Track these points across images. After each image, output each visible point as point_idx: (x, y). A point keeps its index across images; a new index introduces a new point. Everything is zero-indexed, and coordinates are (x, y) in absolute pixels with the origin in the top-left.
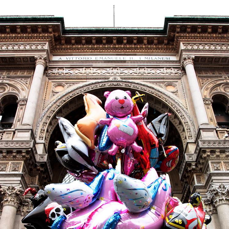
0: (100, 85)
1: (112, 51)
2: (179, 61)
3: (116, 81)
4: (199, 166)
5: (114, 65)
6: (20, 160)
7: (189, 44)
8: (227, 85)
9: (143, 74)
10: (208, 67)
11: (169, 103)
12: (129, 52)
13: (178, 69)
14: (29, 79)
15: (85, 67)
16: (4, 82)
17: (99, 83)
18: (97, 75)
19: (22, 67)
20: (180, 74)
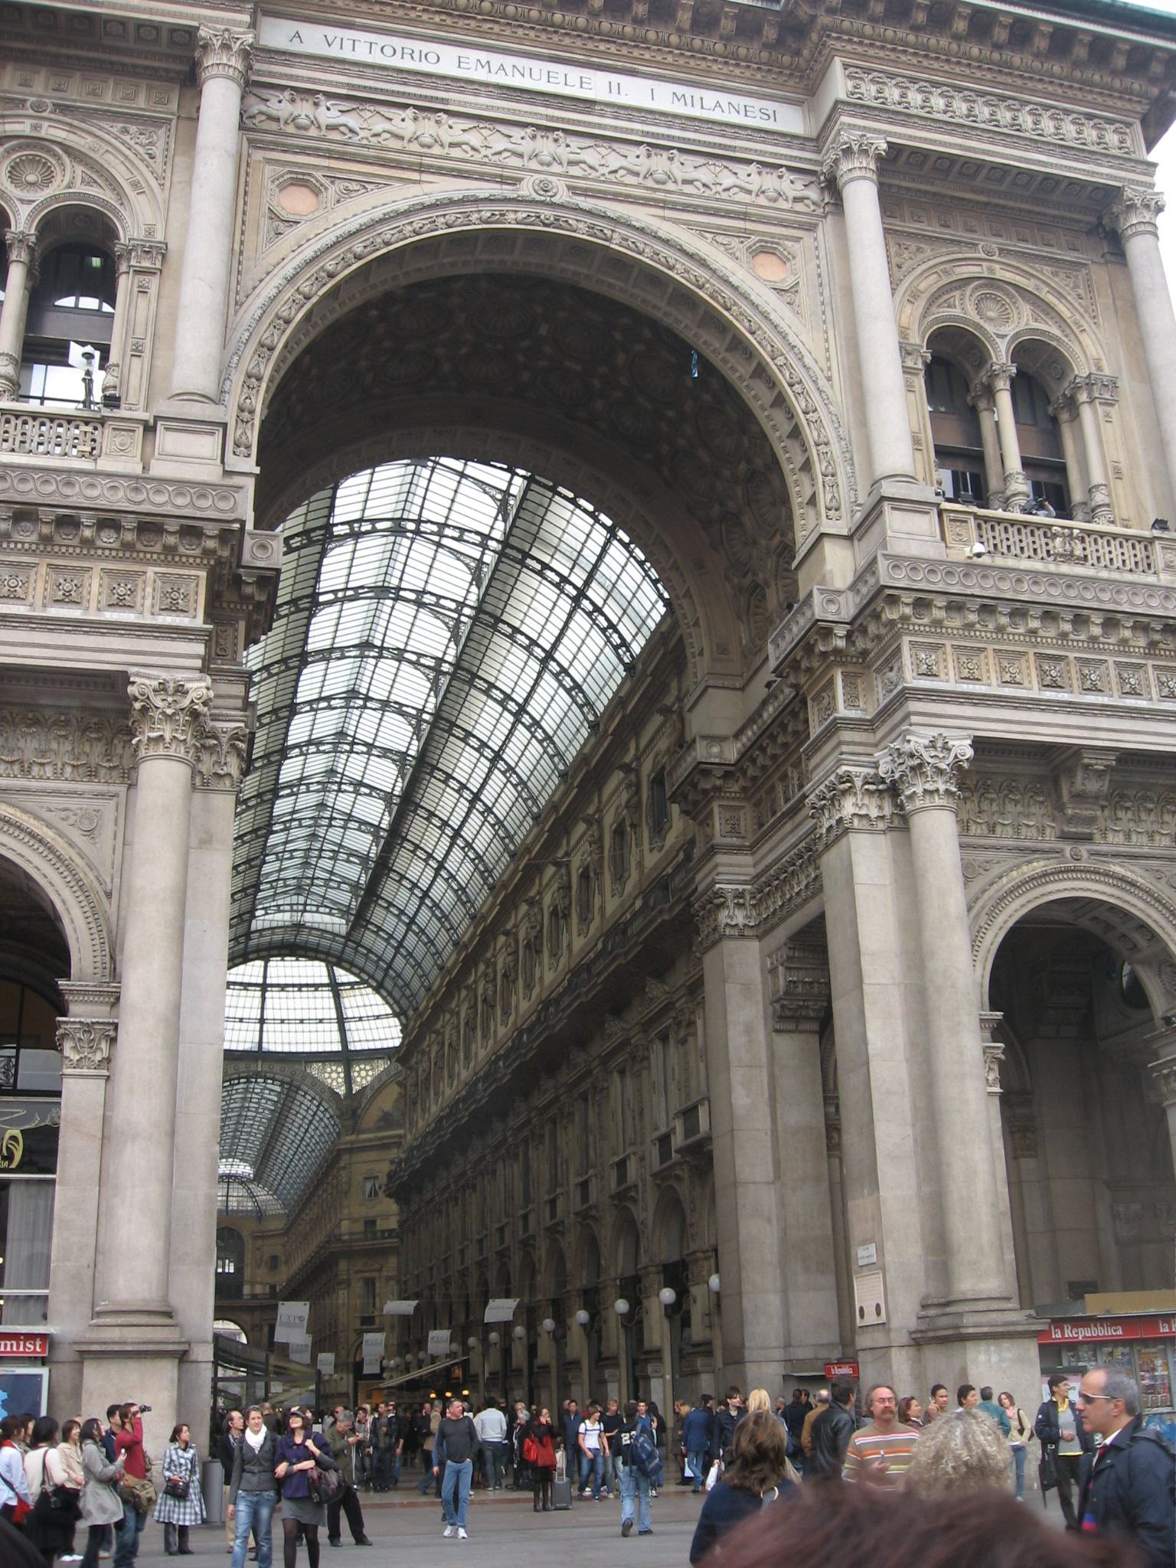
0: (486, 215)
1: (532, 34)
2: (817, 139)
3: (553, 205)
4: (861, 644)
5: (541, 113)
6: (191, 566)
7: (868, 71)
8: (992, 287)
9: (664, 183)
10: (926, 192)
11: (764, 343)
12: (606, 54)
13: (809, 179)
14: (162, 132)
15: (415, 107)
16: (42, 134)
17: (477, 201)
18: (467, 156)
19: (123, 65)
20: (813, 207)
